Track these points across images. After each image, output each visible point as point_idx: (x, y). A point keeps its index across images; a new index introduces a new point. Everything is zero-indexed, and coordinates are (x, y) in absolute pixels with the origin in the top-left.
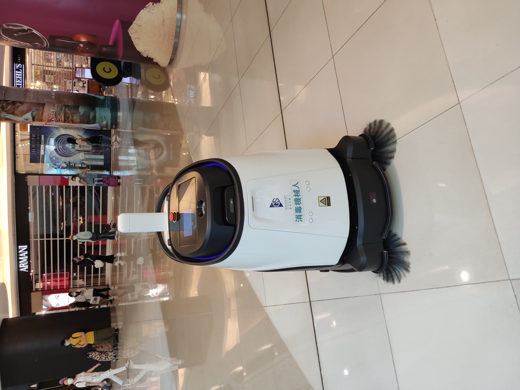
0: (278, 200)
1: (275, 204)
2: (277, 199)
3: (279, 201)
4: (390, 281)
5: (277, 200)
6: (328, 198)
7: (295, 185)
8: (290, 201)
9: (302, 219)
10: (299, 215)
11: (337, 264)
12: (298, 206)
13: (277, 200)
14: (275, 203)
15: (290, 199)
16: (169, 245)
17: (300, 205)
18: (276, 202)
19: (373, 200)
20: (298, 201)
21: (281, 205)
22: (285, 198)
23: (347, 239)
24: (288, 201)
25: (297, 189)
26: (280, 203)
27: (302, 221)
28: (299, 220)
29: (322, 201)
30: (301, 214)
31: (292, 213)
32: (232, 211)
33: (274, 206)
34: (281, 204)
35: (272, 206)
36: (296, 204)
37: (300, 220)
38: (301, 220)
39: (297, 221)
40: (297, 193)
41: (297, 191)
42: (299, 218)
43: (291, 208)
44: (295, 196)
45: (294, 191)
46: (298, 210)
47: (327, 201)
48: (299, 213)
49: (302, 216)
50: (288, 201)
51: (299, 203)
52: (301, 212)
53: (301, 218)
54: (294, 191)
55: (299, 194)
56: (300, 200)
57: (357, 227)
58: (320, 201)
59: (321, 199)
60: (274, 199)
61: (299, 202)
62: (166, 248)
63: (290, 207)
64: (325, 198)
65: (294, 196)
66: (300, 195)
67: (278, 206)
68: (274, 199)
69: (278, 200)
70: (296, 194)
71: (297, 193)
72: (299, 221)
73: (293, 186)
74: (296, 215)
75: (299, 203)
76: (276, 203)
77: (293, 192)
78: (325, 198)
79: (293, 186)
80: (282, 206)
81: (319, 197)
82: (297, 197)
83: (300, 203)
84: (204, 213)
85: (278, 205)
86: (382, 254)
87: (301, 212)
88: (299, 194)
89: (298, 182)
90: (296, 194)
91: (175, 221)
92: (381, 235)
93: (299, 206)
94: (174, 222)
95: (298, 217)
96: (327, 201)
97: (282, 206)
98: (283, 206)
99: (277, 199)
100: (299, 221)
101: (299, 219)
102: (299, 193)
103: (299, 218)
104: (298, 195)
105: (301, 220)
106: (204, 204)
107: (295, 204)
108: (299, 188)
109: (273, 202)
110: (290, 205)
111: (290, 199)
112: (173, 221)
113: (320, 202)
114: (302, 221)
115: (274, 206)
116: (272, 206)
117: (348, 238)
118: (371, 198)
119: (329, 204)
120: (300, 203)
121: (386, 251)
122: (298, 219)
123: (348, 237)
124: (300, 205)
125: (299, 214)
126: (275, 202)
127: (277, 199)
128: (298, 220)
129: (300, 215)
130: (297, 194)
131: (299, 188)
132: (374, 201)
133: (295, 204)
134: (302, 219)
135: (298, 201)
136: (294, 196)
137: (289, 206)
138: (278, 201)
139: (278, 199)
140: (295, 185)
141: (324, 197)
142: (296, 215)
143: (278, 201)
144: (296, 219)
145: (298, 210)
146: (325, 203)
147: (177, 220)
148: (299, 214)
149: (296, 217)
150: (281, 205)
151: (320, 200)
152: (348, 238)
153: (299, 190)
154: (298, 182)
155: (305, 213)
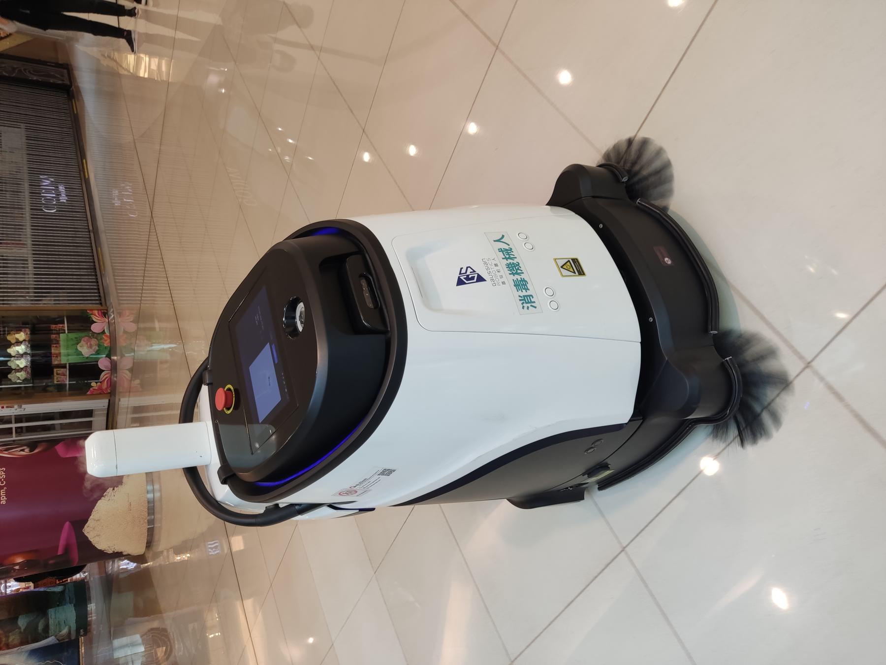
0: (471, 268)
1: (468, 278)
2: (469, 269)
3: (474, 271)
4: (759, 435)
5: (469, 270)
6: (575, 261)
7: (498, 241)
8: (497, 268)
9: (534, 302)
10: (527, 296)
11: (630, 421)
12: (517, 277)
13: (469, 270)
14: (466, 277)
15: (496, 265)
16: (224, 482)
17: (523, 276)
18: (468, 273)
19: (664, 259)
20: (514, 268)
21: (480, 279)
22: (485, 263)
23: (639, 345)
24: (493, 270)
25: (507, 247)
26: (476, 275)
27: (535, 307)
28: (529, 305)
29: (565, 267)
30: (528, 293)
31: (510, 294)
32: (371, 305)
33: (467, 282)
34: (479, 276)
35: (460, 282)
36: (514, 274)
37: (531, 306)
38: (532, 304)
39: (526, 308)
40: (507, 253)
41: (507, 250)
42: (527, 300)
43: (503, 283)
44: (507, 259)
45: (501, 250)
46: (521, 285)
47: (575, 267)
48: (524, 291)
49: (533, 298)
50: (493, 270)
51: (519, 271)
52: (529, 290)
53: (533, 300)
54: (501, 250)
55: (514, 255)
56: (519, 264)
57: (651, 320)
58: (562, 267)
59: (561, 263)
60: (461, 269)
61: (518, 269)
62: (215, 502)
63: (502, 280)
64: (569, 261)
65: (503, 259)
66: (516, 258)
67: (475, 280)
68: (461, 269)
69: (471, 268)
70: (507, 256)
71: (507, 253)
72: (530, 308)
73: (494, 241)
74: (520, 296)
75: (519, 271)
76: (468, 276)
77: (500, 251)
78: (569, 261)
79: (494, 241)
80: (483, 280)
81: (555, 259)
82: (510, 261)
83: (520, 272)
84: (300, 328)
85: (474, 279)
86: (723, 367)
87: (529, 290)
88: (514, 255)
89: (503, 236)
90: (507, 256)
91: (228, 409)
92: (706, 331)
93: (521, 277)
94: (229, 412)
95: (524, 300)
96: (575, 267)
97: (483, 280)
98: (485, 280)
99: (469, 269)
100: (530, 308)
101: (528, 303)
102: (512, 253)
103: (527, 300)
104: (512, 256)
105: (532, 304)
106: (301, 307)
107: (510, 274)
108: (509, 245)
109: (460, 274)
110: (501, 277)
111: (496, 265)
112: (224, 409)
113: (561, 269)
114: (535, 307)
115: (467, 282)
116: (460, 282)
117: (642, 343)
118: (660, 257)
119: (581, 273)
120: (520, 272)
121: (731, 357)
122: (526, 303)
123: (640, 341)
124: (523, 276)
125: (524, 293)
126: (466, 273)
127: (467, 268)
128: (524, 305)
129: (530, 296)
130: (508, 255)
131: (509, 245)
132: (668, 261)
133: (510, 274)
134: (534, 302)
135: (514, 268)
136: (503, 259)
137: (499, 277)
138: (472, 271)
139: (470, 267)
140: (498, 241)
141: (567, 260)
142: (520, 296)
143: (472, 271)
144: (523, 304)
145: (521, 285)
146: (571, 270)
147: (236, 408)
148: (524, 293)
149: (520, 300)
150: (480, 279)
151: (560, 265)
152: (641, 343)
153: (511, 249)
154: (503, 236)
155: (536, 288)
